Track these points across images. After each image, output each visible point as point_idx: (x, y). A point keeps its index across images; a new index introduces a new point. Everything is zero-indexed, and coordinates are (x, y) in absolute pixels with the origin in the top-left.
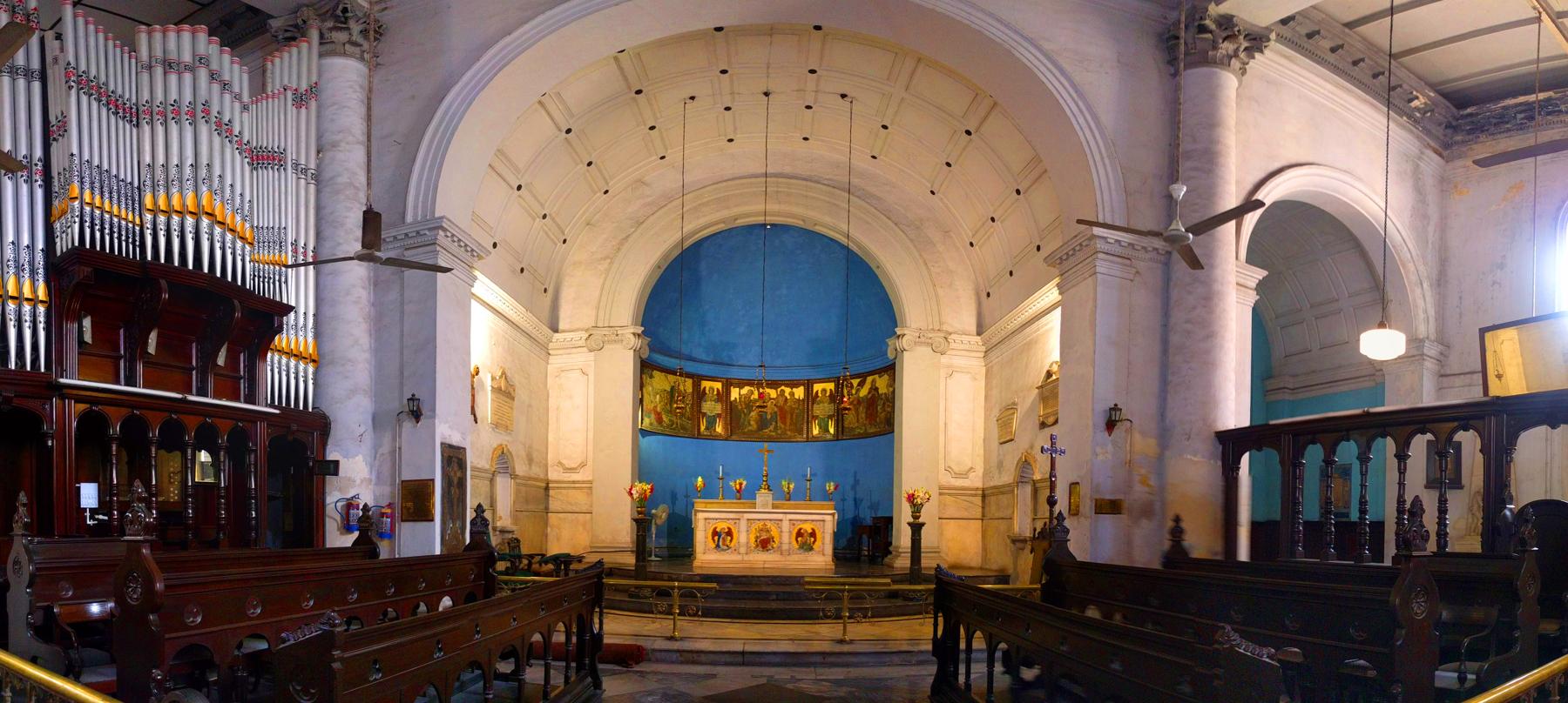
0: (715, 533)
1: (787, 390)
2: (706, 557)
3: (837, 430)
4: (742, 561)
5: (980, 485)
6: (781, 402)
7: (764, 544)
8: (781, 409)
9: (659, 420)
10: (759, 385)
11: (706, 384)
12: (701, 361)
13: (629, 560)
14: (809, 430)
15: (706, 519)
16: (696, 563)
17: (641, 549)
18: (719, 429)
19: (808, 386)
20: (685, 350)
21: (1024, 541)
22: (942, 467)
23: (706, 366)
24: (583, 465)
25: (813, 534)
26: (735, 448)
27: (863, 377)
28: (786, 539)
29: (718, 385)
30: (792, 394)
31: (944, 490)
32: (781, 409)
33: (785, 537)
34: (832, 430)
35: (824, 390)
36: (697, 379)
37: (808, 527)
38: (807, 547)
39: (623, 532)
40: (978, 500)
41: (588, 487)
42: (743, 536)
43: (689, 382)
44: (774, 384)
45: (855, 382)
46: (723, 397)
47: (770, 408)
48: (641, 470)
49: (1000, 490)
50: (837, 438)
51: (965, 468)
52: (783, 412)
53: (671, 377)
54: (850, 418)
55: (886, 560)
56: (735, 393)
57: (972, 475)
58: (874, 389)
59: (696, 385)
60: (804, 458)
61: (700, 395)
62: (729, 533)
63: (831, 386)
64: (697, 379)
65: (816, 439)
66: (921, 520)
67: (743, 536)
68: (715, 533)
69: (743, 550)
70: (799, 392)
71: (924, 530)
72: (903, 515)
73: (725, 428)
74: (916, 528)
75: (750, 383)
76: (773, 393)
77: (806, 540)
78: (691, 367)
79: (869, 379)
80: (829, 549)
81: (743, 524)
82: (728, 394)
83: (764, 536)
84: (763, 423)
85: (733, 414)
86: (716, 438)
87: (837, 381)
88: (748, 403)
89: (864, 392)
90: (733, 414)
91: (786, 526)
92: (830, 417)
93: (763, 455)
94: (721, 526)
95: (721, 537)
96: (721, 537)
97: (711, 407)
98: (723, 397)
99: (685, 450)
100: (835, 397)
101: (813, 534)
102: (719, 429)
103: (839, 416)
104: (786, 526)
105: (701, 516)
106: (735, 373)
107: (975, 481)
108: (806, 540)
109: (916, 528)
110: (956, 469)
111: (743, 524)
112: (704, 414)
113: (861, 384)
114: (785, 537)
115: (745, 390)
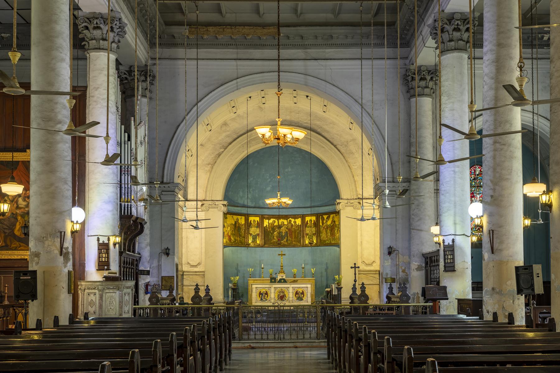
0: (260, 294)
1: (293, 220)
3: (317, 241)
6: (290, 227)
7: (282, 297)
8: (289, 230)
9: (230, 239)
10: (279, 217)
11: (251, 219)
14: (304, 241)
15: (256, 288)
18: (258, 242)
19: (303, 217)
20: (241, 202)
23: (252, 209)
24: (199, 264)
25: (303, 293)
28: (291, 295)
29: (257, 219)
30: (295, 222)
32: (289, 230)
33: (290, 295)
34: (315, 241)
35: (311, 220)
36: (247, 216)
37: (300, 290)
41: (202, 274)
43: (243, 218)
44: (286, 217)
45: (325, 217)
46: (260, 225)
47: (283, 229)
51: (370, 262)
52: (290, 230)
53: (235, 217)
54: (323, 236)
56: (266, 223)
57: (374, 264)
58: (334, 221)
59: (247, 220)
61: (248, 225)
62: (266, 293)
63: (314, 218)
64: (247, 216)
68: (260, 294)
70: (299, 221)
76: (286, 222)
77: (299, 295)
78: (244, 211)
79: (332, 216)
80: (309, 300)
83: (282, 294)
84: (280, 237)
85: (267, 233)
87: (318, 216)
88: (273, 228)
89: (329, 223)
90: (267, 233)
91: (291, 290)
92: (314, 234)
95: (263, 295)
96: (263, 295)
97: (254, 230)
99: (241, 254)
100: (316, 224)
103: (318, 233)
104: (291, 290)
105: (254, 286)
106: (266, 212)
108: (299, 295)
110: (367, 262)
112: (251, 234)
114: (290, 295)
115: (271, 221)
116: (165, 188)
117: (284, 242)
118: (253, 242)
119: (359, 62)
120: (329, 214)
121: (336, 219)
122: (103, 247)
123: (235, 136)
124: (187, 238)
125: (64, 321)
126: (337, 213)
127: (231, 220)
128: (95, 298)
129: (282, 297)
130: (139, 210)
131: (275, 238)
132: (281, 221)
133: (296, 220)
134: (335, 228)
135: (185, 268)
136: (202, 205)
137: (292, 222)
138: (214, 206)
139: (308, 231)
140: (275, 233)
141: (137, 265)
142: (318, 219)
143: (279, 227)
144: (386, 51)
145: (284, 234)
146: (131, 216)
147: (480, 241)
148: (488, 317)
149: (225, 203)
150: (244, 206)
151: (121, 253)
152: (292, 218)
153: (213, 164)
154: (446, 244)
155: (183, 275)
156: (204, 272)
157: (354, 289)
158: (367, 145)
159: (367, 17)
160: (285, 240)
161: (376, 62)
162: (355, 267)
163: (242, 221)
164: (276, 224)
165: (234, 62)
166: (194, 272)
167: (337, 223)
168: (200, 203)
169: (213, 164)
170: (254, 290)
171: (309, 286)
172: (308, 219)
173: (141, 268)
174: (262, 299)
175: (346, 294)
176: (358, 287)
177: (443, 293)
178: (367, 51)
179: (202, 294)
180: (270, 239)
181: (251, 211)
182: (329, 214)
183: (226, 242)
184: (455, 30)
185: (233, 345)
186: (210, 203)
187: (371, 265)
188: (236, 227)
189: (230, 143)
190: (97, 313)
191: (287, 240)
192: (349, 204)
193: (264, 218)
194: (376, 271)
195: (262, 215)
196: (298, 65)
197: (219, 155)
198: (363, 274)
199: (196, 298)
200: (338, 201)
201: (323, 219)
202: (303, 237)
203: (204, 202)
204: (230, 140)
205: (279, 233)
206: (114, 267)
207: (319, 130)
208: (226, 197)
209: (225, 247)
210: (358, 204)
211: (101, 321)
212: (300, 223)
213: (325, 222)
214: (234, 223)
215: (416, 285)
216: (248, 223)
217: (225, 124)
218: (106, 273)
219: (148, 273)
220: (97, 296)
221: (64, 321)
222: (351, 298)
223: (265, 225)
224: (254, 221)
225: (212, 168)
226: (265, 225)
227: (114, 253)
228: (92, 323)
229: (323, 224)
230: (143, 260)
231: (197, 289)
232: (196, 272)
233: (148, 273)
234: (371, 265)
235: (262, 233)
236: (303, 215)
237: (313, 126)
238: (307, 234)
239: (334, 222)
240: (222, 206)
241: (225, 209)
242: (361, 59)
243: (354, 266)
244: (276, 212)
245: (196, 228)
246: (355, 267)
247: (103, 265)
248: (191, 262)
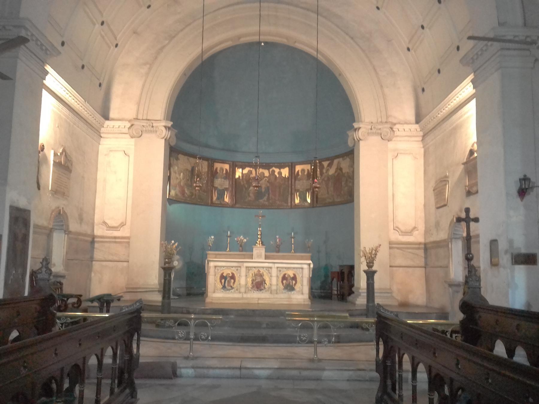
0: (222, 277)
1: (277, 170)
3: (312, 199)
4: (243, 298)
5: (421, 239)
7: (259, 284)
9: (183, 193)
11: (218, 166)
12: (214, 148)
13: (158, 298)
14: (293, 199)
15: (216, 266)
16: (208, 300)
17: (166, 289)
18: (227, 199)
21: (458, 285)
22: (391, 227)
24: (123, 225)
25: (294, 278)
27: (331, 159)
29: (227, 167)
30: (280, 173)
31: (392, 245)
33: (273, 280)
34: (309, 200)
35: (303, 170)
37: (291, 273)
38: (290, 288)
39: (153, 278)
40: (421, 253)
41: (126, 241)
42: (244, 280)
43: (205, 164)
44: (267, 166)
45: (325, 164)
47: (263, 184)
48: (169, 230)
49: (438, 245)
50: (313, 205)
51: (410, 228)
55: (350, 298)
56: (239, 173)
57: (416, 233)
59: (210, 166)
61: (213, 174)
62: (233, 277)
63: (307, 167)
64: (211, 161)
65: (297, 207)
66: (374, 268)
67: (244, 280)
68: (222, 277)
69: (243, 290)
70: (285, 172)
71: (376, 277)
72: (361, 267)
73: (231, 198)
74: (370, 275)
75: (250, 165)
76: (266, 173)
79: (336, 161)
80: (306, 289)
81: (243, 271)
82: (234, 173)
83: (259, 279)
84: (259, 195)
86: (225, 205)
89: (332, 172)
90: (238, 188)
91: (274, 272)
94: (227, 272)
95: (227, 281)
96: (227, 281)
100: (312, 175)
101: (294, 278)
102: (227, 199)
104: (274, 272)
105: (212, 264)
106: (240, 158)
107: (418, 237)
109: (370, 275)
110: (403, 229)
111: (243, 270)
112: (216, 188)
113: (330, 165)
114: (273, 280)
115: (246, 171)
117: (263, 201)
118: (218, 199)
124: (105, 180)
129: (259, 284)
131: (251, 195)
132: (261, 170)
133: (282, 170)
135: (99, 231)
136: (132, 125)
137: (276, 174)
138: (150, 128)
139: (300, 185)
140: (251, 188)
143: (257, 179)
145: (263, 190)
150: (207, 146)
152: (276, 167)
155: (93, 242)
156: (128, 238)
160: (265, 198)
163: (204, 167)
164: (254, 175)
166: (112, 238)
167: (346, 170)
171: (306, 266)
172: (298, 168)
174: (224, 287)
183: (176, 195)
186: (144, 123)
191: (268, 199)
192: (374, 130)
193: (236, 166)
194: (420, 244)
195: (233, 162)
198: (398, 248)
202: (292, 194)
210: (388, 130)
212: (287, 175)
213: (324, 171)
214: (190, 169)
216: (212, 171)
223: (237, 176)
224: (222, 169)
225: (150, 69)
226: (237, 176)
229: (321, 173)
232: (115, 238)
234: (409, 233)
235: (232, 187)
236: (292, 163)
238: (298, 191)
239: (341, 169)
240: (164, 129)
243: (472, 216)
248: (108, 222)
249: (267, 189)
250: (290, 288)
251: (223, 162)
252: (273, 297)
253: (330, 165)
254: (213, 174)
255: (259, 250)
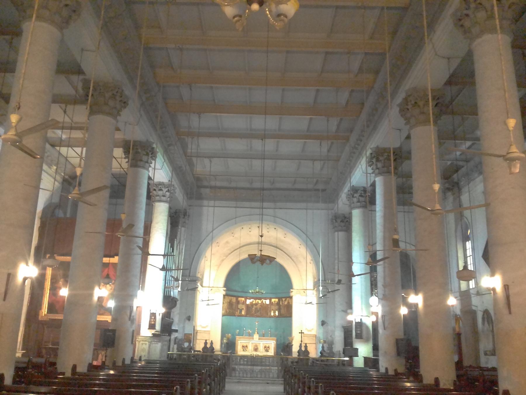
0: (243, 346)
1: (264, 301)
2: (240, 352)
5: (315, 333)
7: (256, 349)
9: (226, 311)
10: (256, 299)
11: (240, 299)
14: (270, 314)
15: (240, 342)
24: (207, 326)
25: (269, 347)
26: (248, 319)
29: (243, 299)
33: (261, 348)
40: (315, 338)
41: (208, 332)
42: (251, 347)
43: (235, 298)
44: (260, 299)
45: (284, 299)
50: (278, 317)
53: (230, 297)
54: (283, 311)
58: (288, 303)
59: (237, 299)
60: (269, 323)
62: (247, 347)
63: (277, 300)
67: (251, 347)
68: (243, 346)
76: (260, 302)
86: (241, 316)
87: (280, 299)
89: (286, 303)
90: (249, 308)
93: (256, 322)
94: (245, 345)
95: (245, 348)
96: (245, 348)
97: (240, 306)
98: (244, 303)
108: (267, 349)
113: (285, 300)
114: (261, 348)
115: (252, 300)
116: (190, 281)
119: (305, 211)
120: (286, 298)
121: (290, 301)
122: (153, 315)
123: (233, 250)
125: (128, 362)
126: (291, 298)
127: (228, 299)
128: (146, 347)
129: (256, 349)
130: (175, 293)
132: (257, 300)
134: (289, 308)
135: (198, 329)
141: (171, 327)
142: (279, 301)
143: (256, 304)
144: (321, 205)
146: (170, 296)
147: (377, 321)
148: (382, 370)
149: (225, 289)
150: (236, 291)
151: (163, 319)
153: (219, 266)
154: (357, 321)
155: (197, 333)
157: (301, 346)
158: (309, 258)
159: (310, 186)
161: (315, 211)
162: (301, 333)
163: (234, 300)
164: (254, 303)
165: (234, 209)
168: (210, 289)
169: (219, 266)
170: (239, 344)
171: (273, 343)
173: (173, 328)
175: (295, 349)
176: (303, 345)
177: (355, 353)
178: (310, 205)
179: (208, 346)
180: (251, 311)
181: (239, 294)
182: (286, 298)
184: (360, 196)
185: (227, 380)
187: (310, 331)
188: (230, 304)
189: (230, 254)
190: (146, 357)
191: (261, 313)
196: (271, 211)
197: (223, 260)
199: (205, 348)
200: (292, 290)
201: (282, 300)
203: (213, 288)
204: (229, 252)
205: (256, 309)
206: (158, 327)
207: (281, 248)
208: (225, 286)
209: (223, 315)
211: (148, 362)
215: (339, 346)
217: (227, 242)
218: (153, 331)
219: (176, 331)
220: (147, 345)
221: (128, 362)
222: (299, 352)
227: (159, 318)
228: (143, 363)
230: (174, 323)
231: (206, 343)
233: (176, 331)
234: (310, 331)
237: (278, 246)
241: (224, 293)
242: (306, 209)
244: (255, 296)
245: (208, 305)
246: (301, 333)
247: (152, 326)
249: (260, 309)
250: (267, 351)
251: (242, 297)
252: (261, 352)
253: (285, 300)
254: (238, 302)
255: (256, 336)
